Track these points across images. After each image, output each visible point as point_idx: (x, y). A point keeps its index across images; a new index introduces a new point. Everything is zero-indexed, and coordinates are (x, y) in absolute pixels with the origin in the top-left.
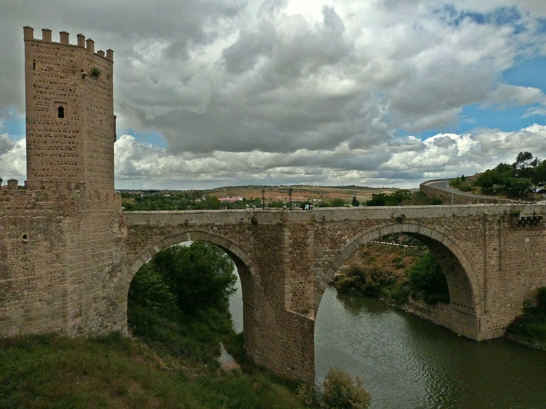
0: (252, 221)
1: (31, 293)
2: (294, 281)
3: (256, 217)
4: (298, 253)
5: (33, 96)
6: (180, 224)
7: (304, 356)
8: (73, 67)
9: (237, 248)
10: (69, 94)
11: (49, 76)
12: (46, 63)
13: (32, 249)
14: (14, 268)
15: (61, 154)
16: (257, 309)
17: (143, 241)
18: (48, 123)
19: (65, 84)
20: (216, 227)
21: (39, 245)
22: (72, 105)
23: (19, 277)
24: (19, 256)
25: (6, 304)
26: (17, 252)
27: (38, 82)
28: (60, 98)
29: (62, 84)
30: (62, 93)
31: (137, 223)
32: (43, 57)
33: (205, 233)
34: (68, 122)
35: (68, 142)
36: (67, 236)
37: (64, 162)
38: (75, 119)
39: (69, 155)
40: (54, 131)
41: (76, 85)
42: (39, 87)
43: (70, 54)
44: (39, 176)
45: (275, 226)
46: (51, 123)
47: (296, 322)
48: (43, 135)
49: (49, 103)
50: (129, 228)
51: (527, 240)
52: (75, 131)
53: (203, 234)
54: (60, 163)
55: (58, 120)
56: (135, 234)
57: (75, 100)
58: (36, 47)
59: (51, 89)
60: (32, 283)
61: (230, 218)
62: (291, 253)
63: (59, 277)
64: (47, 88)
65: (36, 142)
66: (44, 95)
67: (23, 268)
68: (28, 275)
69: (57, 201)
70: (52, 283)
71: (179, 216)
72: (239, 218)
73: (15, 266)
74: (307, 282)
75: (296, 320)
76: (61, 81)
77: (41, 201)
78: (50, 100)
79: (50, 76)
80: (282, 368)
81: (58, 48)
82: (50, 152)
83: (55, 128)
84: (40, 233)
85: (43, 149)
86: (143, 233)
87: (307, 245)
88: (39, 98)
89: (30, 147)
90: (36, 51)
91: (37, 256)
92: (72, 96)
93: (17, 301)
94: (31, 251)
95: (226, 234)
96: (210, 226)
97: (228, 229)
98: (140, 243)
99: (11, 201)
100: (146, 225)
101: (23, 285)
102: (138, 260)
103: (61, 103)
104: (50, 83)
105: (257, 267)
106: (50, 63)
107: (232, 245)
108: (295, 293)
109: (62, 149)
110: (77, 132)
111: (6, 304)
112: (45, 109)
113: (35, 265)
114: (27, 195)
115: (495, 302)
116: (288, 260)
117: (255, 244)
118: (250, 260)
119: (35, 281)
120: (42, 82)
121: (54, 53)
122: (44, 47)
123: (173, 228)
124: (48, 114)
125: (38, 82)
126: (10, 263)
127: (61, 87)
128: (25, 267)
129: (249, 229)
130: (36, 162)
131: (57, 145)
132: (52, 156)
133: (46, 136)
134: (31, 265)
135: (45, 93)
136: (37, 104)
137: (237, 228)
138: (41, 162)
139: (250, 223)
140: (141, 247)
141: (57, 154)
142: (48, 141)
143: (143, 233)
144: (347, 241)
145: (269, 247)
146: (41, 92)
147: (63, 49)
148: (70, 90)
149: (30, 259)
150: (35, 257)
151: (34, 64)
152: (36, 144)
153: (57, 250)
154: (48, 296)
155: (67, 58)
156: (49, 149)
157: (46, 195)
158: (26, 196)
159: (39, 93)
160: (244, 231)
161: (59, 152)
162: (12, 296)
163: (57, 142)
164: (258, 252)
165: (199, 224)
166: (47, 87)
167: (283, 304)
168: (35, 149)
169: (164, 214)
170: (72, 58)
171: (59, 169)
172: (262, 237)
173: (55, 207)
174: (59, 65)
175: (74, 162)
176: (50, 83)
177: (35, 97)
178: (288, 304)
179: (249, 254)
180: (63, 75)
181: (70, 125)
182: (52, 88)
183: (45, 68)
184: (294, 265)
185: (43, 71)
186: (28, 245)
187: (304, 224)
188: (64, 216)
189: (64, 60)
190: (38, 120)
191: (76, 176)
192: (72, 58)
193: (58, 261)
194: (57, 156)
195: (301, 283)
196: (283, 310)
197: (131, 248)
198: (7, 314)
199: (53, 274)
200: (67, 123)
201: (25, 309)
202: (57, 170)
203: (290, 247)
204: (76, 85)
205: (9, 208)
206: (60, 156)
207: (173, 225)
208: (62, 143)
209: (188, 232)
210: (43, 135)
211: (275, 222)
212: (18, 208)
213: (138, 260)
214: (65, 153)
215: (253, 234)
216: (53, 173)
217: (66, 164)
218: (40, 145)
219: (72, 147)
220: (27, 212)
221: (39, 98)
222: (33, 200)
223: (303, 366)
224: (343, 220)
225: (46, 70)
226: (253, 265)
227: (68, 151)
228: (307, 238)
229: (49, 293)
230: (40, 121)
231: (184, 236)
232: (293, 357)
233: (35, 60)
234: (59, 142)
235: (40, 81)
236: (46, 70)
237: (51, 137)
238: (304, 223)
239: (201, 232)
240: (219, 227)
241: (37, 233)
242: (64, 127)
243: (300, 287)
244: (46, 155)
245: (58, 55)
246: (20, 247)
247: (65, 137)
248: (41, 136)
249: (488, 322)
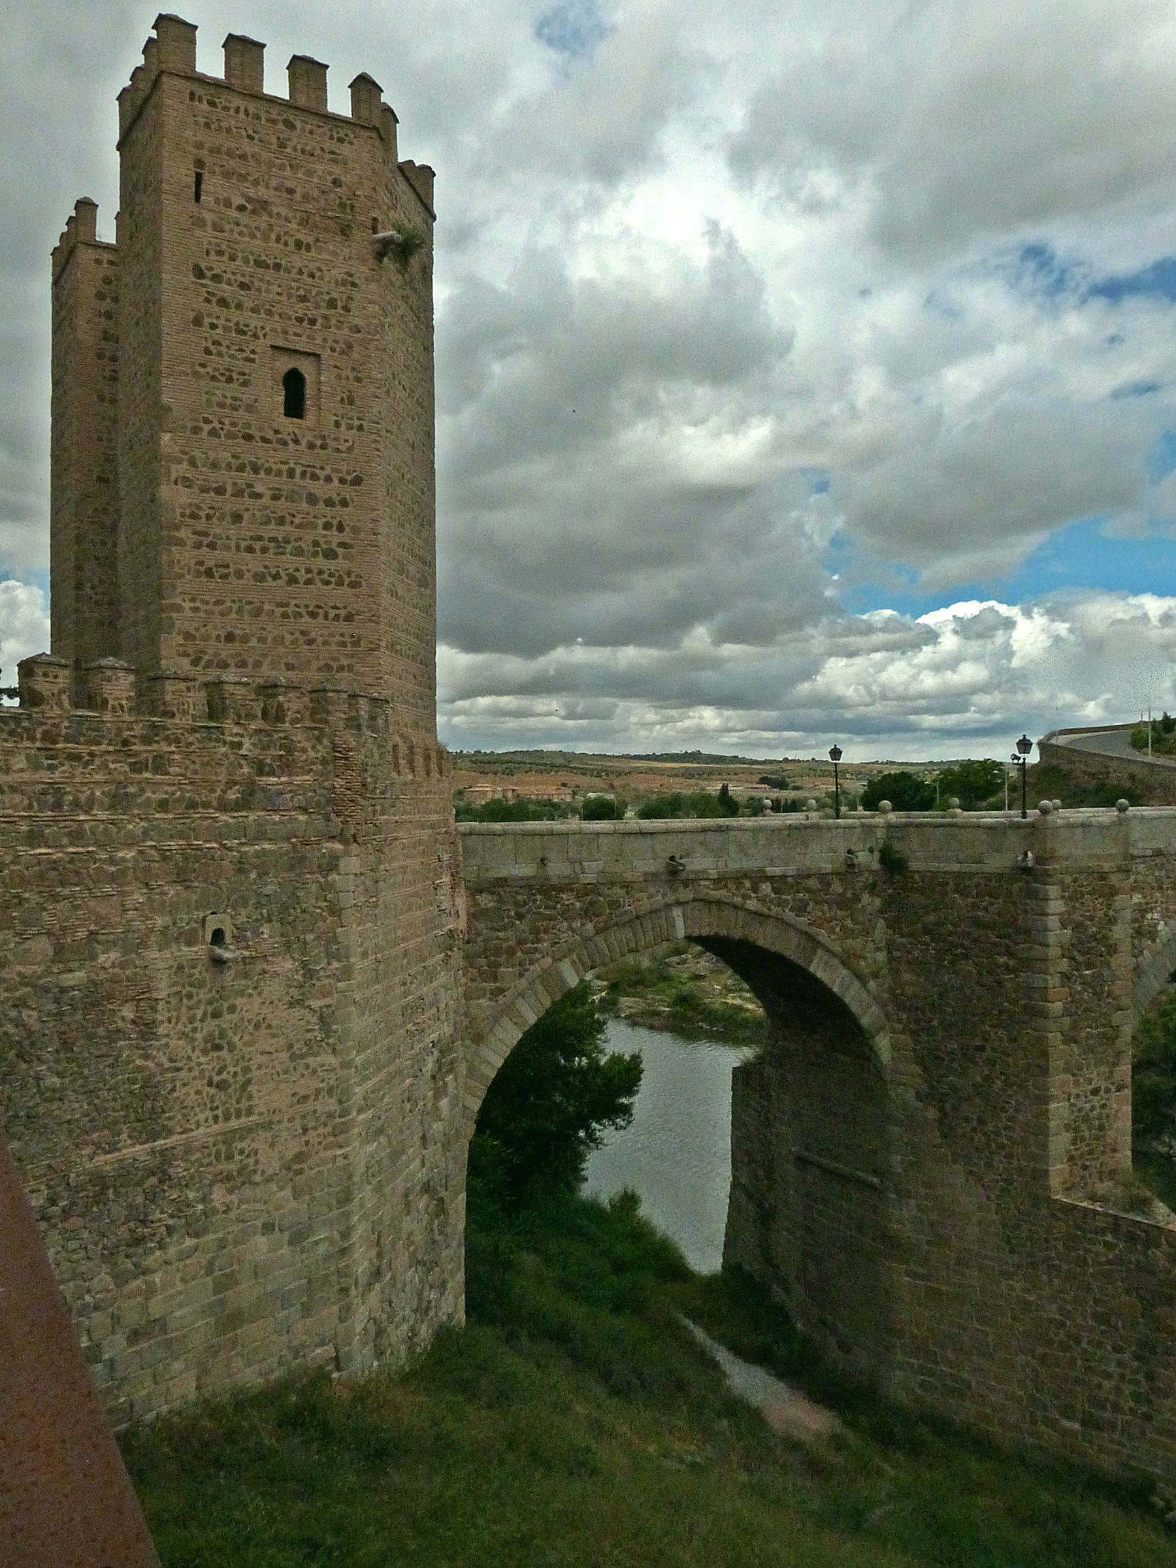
0: (882, 861)
1: (234, 1198)
2: (1077, 1084)
3: (897, 846)
4: (1089, 980)
5: (192, 315)
6: (653, 874)
7: (1150, 1377)
8: (342, 206)
9: (836, 962)
10: (325, 318)
11: (253, 236)
12: (243, 178)
13: (242, 993)
14: (178, 1083)
15: (297, 574)
17: (521, 942)
18: (248, 437)
19: (312, 276)
20: (769, 884)
21: (264, 972)
22: (336, 367)
23: (198, 1125)
24: (195, 1030)
25: (149, 1261)
26: (190, 1008)
27: (213, 256)
28: (296, 335)
29: (300, 272)
30: (300, 314)
31: (504, 873)
32: (230, 153)
33: (735, 907)
34: (323, 438)
35: (320, 522)
36: (353, 933)
37: (307, 606)
38: (350, 427)
39: (325, 576)
40: (268, 471)
41: (354, 285)
42: (217, 278)
43: (333, 153)
44: (208, 665)
45: (1000, 877)
46: (257, 435)
47: (1107, 1245)
48: (229, 489)
49: (253, 352)
50: (476, 890)
52: (349, 478)
53: (728, 912)
54: (289, 610)
55: (289, 425)
57: (350, 347)
58: (205, 106)
59: (259, 290)
60: (242, 1152)
61: (815, 847)
62: (1066, 977)
63: (331, 1116)
64: (243, 286)
65: (198, 517)
66: (236, 316)
67: (210, 1084)
68: (227, 1118)
69: (324, 775)
70: (307, 1143)
71: (645, 843)
72: (841, 846)
73: (183, 1074)
74: (1113, 1088)
75: (1109, 1238)
76: (298, 260)
77: (272, 773)
78: (255, 336)
79: (258, 234)
80: (1034, 1423)
81: (290, 126)
82: (253, 563)
83: (272, 458)
84: (270, 921)
85: (228, 548)
86: (523, 910)
87: (1113, 949)
88: (213, 326)
89: (177, 534)
90: (207, 126)
91: (257, 1026)
92: (338, 328)
93: (189, 1242)
94: (239, 1002)
95: (801, 909)
96: (750, 878)
97: (808, 890)
98: (511, 953)
99: (171, 770)
100: (533, 877)
101: (210, 1164)
102: (505, 1021)
103: (297, 356)
104: (259, 264)
105: (903, 1032)
106: (256, 183)
107: (819, 952)
108: (1076, 1130)
109: (299, 552)
110: (357, 481)
111: (149, 1261)
112: (235, 376)
113: (253, 1064)
114: (225, 743)
116: (1057, 1007)
117: (890, 947)
118: (874, 1009)
119: (248, 1141)
120: (225, 258)
121: (274, 140)
122: (237, 111)
123: (627, 886)
124: (246, 395)
125: (213, 256)
126: (167, 1065)
127: (298, 289)
128: (216, 1079)
129: (872, 888)
130: (197, 604)
131: (279, 532)
132: (259, 577)
133: (239, 493)
134: (238, 1069)
135: (239, 306)
136: (208, 352)
137: (837, 887)
138: (217, 603)
139: (876, 866)
140: (513, 966)
141: (282, 573)
142: (246, 516)
143: (523, 910)
144: (1159, 928)
145: (966, 957)
146: (223, 302)
147: (308, 127)
148: (332, 304)
149: (236, 1039)
150: (251, 1028)
151: (199, 178)
152: (201, 525)
153: (325, 994)
154: (293, 1204)
155: (319, 167)
156: (250, 550)
157: (288, 747)
158: (223, 750)
159: (214, 304)
160: (857, 899)
161: (288, 562)
162: (172, 1216)
163: (281, 521)
164: (907, 976)
165: (713, 874)
166: (246, 280)
168: (198, 546)
169: (598, 834)
170: (338, 171)
171: (288, 638)
172: (932, 918)
173: (318, 804)
174: (291, 191)
175: (345, 607)
176: (259, 264)
177: (198, 322)
178: (1058, 1172)
179: (872, 985)
180: (305, 237)
181: (329, 450)
182: (264, 287)
183: (238, 201)
184: (1074, 1027)
185: (235, 214)
186: (229, 975)
187: (1106, 870)
188: (346, 843)
189: (310, 173)
190: (207, 421)
191: (350, 668)
192: (338, 171)
193: (328, 1044)
194: (279, 582)
195: (1095, 1092)
196: (1040, 1199)
197: (481, 973)
198: (156, 1308)
199: (309, 1106)
200: (319, 442)
201: (217, 1273)
202: (279, 640)
203: (1063, 956)
204: (354, 285)
205: (163, 806)
206: (293, 580)
207: (628, 876)
208: (299, 526)
209: (678, 903)
210: (229, 489)
211: (997, 863)
212: (192, 805)
213: (505, 1021)
214: (308, 571)
216: (265, 656)
217: (313, 615)
218: (218, 529)
219: (334, 546)
220: (227, 825)
221: (213, 326)
222: (246, 770)
223: (1148, 1418)
224: (1149, 853)
225: (241, 208)
226: (882, 1028)
227: (320, 562)
229: (296, 1194)
230: (217, 426)
231: (663, 922)
232: (1096, 1380)
233: (200, 163)
234: (288, 519)
235: (220, 253)
236: (241, 208)
237: (259, 496)
238: (1106, 867)
239: (719, 903)
240: (780, 883)
241: (257, 920)
242: (309, 458)
243: (1093, 1108)
244: (239, 574)
245: (289, 150)
246: (200, 985)
247: (312, 499)
248: (220, 491)
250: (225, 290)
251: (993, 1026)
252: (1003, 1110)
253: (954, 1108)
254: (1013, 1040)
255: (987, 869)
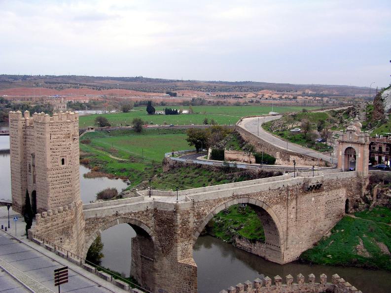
16: (156, 262)
51: (313, 199)
56: (89, 223)
95: (139, 217)
115: (293, 242)
132: (59, 188)
137: (145, 213)
164: (157, 227)
165: (124, 213)
167: (176, 258)
179: (151, 228)
180: (64, 140)
195: (186, 245)
215: (153, 216)
228: (189, 218)
240: (135, 214)
249: (288, 254)
250: (54, 150)
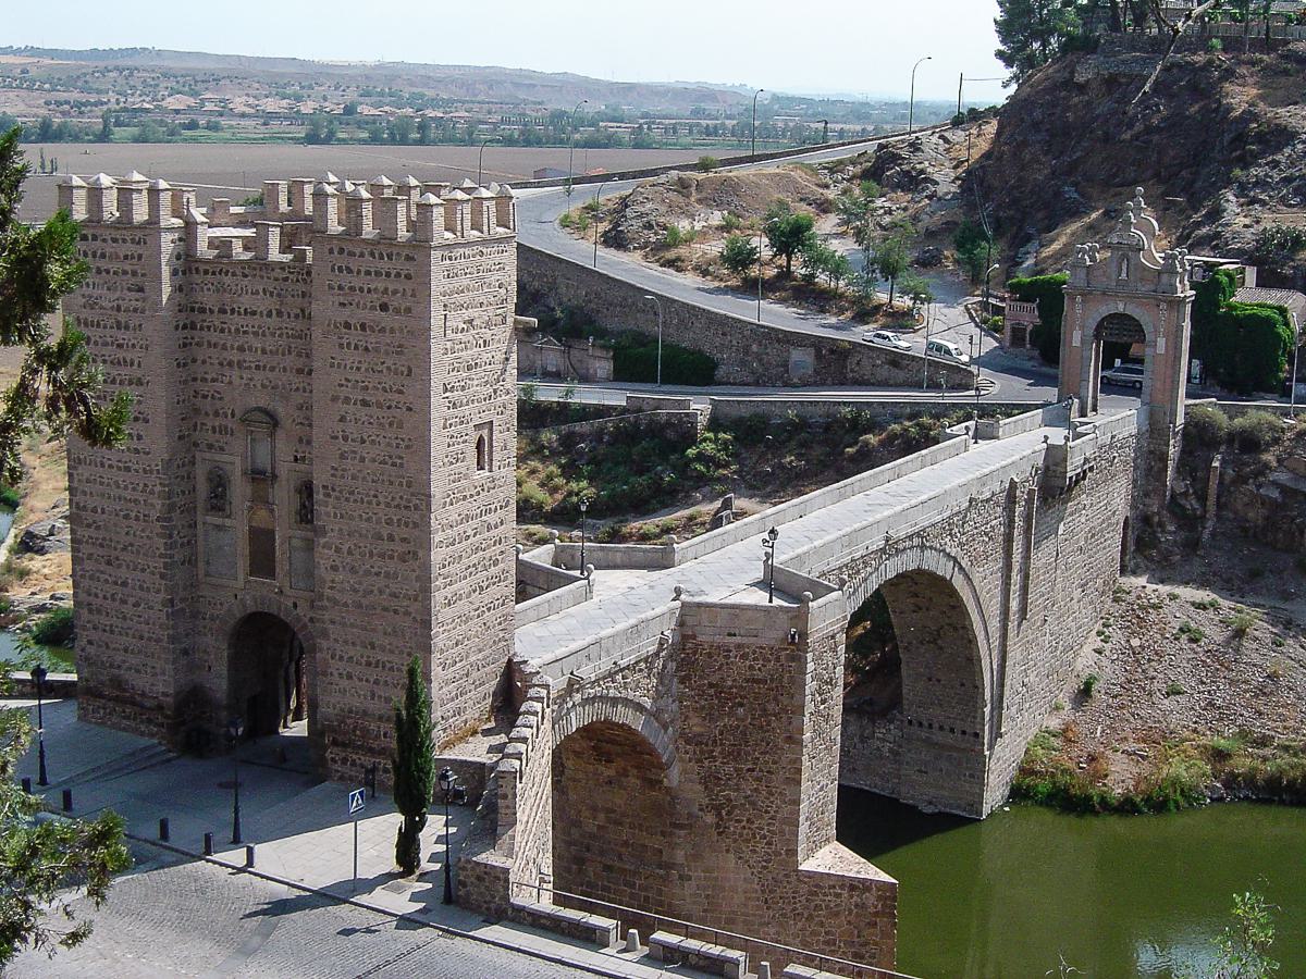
251: (761, 753)
252: (766, 812)
253: (728, 813)
254: (775, 763)
255: (761, 642)
